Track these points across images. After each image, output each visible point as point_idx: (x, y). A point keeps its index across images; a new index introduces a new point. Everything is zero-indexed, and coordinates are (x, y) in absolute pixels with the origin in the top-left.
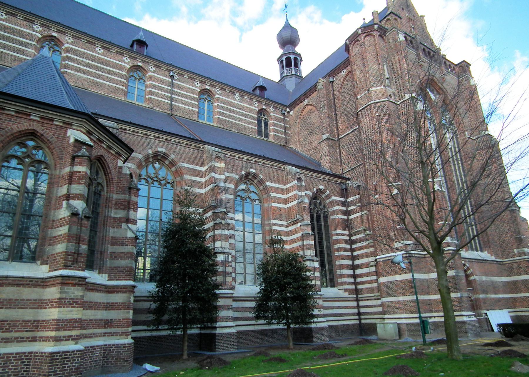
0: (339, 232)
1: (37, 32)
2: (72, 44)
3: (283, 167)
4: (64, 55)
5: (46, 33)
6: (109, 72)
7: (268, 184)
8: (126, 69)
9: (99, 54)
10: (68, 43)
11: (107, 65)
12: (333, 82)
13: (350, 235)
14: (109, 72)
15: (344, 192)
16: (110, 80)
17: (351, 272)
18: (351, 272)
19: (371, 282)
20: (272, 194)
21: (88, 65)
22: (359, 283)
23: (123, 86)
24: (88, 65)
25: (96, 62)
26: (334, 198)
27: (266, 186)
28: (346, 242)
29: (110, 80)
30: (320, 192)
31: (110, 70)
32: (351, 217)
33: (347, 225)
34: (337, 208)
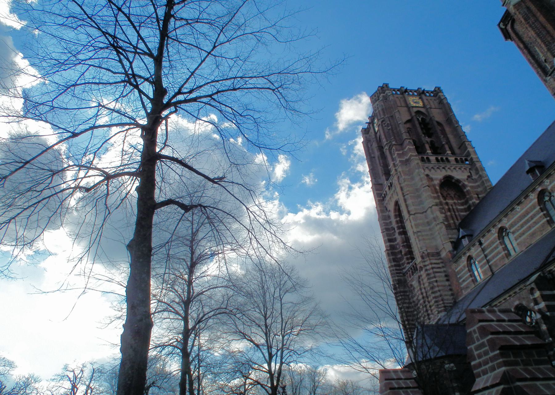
1: (495, 233)
2: (508, 221)
5: (497, 230)
6: (532, 218)
8: (537, 204)
9: (520, 211)
10: (506, 224)
11: (528, 214)
14: (532, 218)
16: (536, 223)
21: (522, 226)
23: (544, 218)
24: (522, 226)
25: (523, 219)
29: (536, 223)
31: (531, 216)
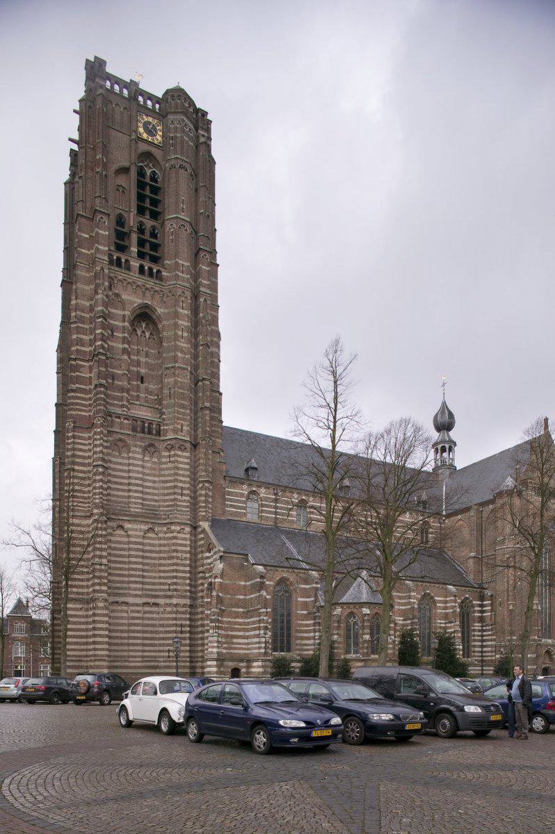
0: (476, 624)
3: (445, 586)
4: (308, 510)
7: (436, 598)
12: (482, 511)
13: (482, 626)
15: (482, 598)
17: (480, 649)
18: (480, 649)
19: (492, 656)
20: (438, 605)
22: (485, 656)
26: (474, 602)
27: (435, 600)
28: (479, 631)
30: (467, 598)
32: (485, 614)
33: (481, 619)
34: (476, 608)
